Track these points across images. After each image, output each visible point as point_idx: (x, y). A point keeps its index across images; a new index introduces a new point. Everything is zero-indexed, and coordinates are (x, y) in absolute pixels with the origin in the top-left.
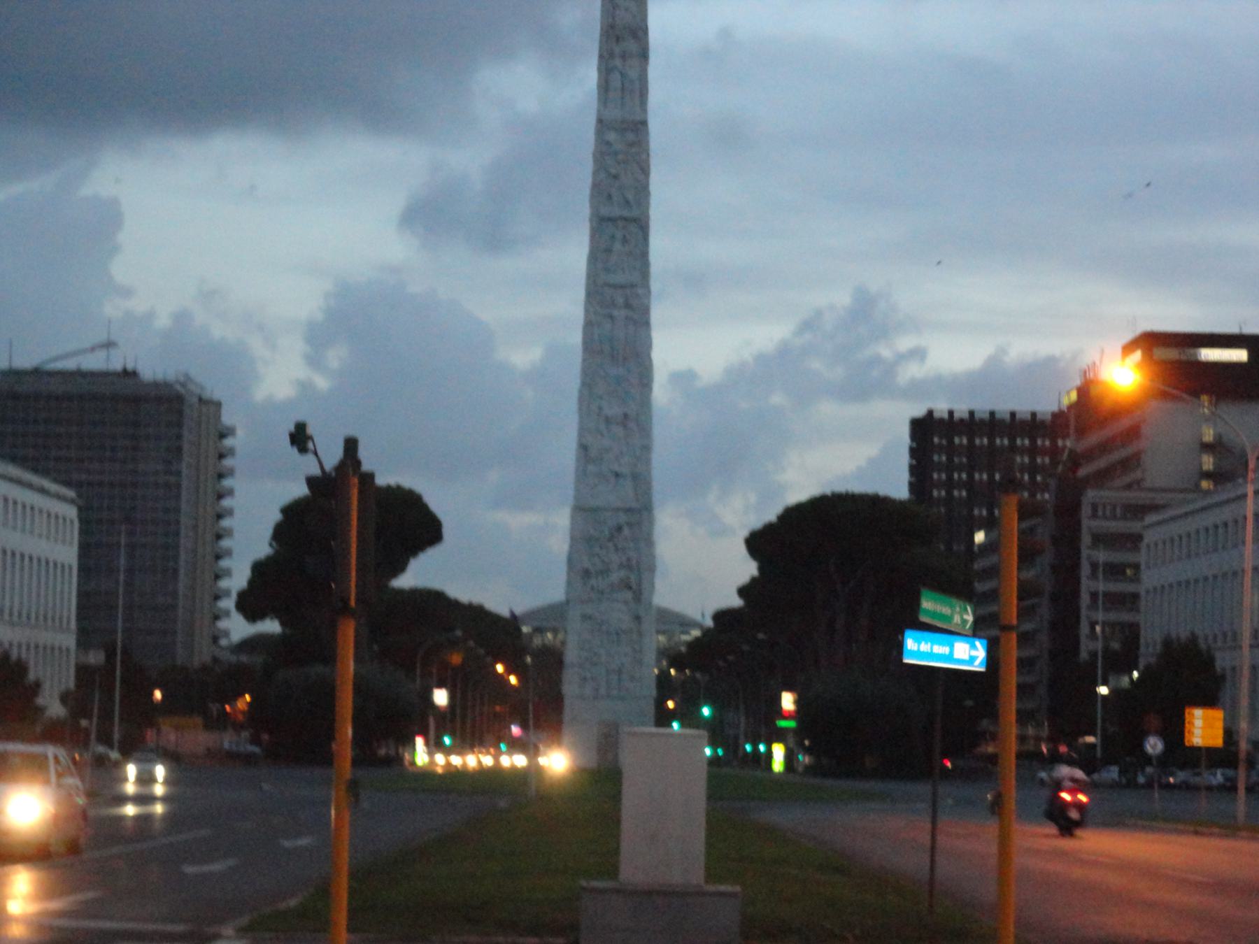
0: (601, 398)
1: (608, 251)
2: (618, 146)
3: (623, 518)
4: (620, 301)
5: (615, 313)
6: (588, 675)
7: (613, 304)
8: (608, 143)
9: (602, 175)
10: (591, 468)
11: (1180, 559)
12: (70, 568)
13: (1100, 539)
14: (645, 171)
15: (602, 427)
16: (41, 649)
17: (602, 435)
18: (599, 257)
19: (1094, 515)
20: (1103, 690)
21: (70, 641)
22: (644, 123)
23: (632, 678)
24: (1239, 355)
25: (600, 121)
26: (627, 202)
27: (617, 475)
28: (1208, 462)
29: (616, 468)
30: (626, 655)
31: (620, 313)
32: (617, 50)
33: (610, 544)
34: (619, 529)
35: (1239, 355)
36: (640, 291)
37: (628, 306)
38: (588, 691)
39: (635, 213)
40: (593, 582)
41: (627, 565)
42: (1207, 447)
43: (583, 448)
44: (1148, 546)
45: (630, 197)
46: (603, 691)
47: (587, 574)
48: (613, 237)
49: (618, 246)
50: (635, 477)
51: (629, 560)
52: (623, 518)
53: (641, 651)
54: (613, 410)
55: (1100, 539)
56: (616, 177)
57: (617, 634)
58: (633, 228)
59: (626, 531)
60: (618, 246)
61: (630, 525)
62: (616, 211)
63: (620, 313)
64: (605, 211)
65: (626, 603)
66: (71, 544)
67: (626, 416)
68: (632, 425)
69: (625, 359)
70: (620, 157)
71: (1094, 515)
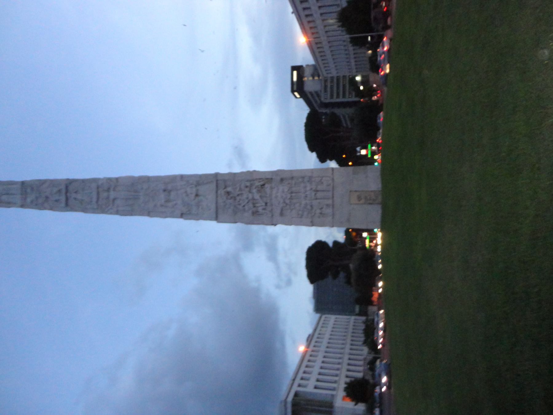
1: (81, 201)
4: (105, 194)
6: (318, 211)
7: (108, 198)
8: (32, 202)
9: (46, 205)
12: (336, 318)
13: (332, 96)
15: (170, 204)
18: (84, 207)
21: (353, 318)
22: (23, 183)
23: (321, 182)
24: (295, 73)
26: (60, 191)
27: (197, 195)
28: (316, 78)
29: (193, 195)
30: (305, 187)
31: (112, 194)
33: (238, 198)
34: (228, 193)
36: (100, 183)
37: (108, 190)
38: (329, 211)
39: (63, 187)
40: (260, 209)
42: (313, 78)
43: (182, 216)
44: (327, 73)
45: (55, 190)
46: (330, 202)
49: (79, 196)
50: (198, 184)
51: (247, 187)
52: (221, 192)
53: (303, 178)
54: (162, 197)
57: (292, 193)
58: (71, 188)
59: (229, 189)
60: (79, 196)
61: (226, 187)
62: (63, 198)
63: (112, 194)
64: (63, 205)
65: (272, 188)
67: (165, 190)
68: (169, 187)
69: (136, 191)
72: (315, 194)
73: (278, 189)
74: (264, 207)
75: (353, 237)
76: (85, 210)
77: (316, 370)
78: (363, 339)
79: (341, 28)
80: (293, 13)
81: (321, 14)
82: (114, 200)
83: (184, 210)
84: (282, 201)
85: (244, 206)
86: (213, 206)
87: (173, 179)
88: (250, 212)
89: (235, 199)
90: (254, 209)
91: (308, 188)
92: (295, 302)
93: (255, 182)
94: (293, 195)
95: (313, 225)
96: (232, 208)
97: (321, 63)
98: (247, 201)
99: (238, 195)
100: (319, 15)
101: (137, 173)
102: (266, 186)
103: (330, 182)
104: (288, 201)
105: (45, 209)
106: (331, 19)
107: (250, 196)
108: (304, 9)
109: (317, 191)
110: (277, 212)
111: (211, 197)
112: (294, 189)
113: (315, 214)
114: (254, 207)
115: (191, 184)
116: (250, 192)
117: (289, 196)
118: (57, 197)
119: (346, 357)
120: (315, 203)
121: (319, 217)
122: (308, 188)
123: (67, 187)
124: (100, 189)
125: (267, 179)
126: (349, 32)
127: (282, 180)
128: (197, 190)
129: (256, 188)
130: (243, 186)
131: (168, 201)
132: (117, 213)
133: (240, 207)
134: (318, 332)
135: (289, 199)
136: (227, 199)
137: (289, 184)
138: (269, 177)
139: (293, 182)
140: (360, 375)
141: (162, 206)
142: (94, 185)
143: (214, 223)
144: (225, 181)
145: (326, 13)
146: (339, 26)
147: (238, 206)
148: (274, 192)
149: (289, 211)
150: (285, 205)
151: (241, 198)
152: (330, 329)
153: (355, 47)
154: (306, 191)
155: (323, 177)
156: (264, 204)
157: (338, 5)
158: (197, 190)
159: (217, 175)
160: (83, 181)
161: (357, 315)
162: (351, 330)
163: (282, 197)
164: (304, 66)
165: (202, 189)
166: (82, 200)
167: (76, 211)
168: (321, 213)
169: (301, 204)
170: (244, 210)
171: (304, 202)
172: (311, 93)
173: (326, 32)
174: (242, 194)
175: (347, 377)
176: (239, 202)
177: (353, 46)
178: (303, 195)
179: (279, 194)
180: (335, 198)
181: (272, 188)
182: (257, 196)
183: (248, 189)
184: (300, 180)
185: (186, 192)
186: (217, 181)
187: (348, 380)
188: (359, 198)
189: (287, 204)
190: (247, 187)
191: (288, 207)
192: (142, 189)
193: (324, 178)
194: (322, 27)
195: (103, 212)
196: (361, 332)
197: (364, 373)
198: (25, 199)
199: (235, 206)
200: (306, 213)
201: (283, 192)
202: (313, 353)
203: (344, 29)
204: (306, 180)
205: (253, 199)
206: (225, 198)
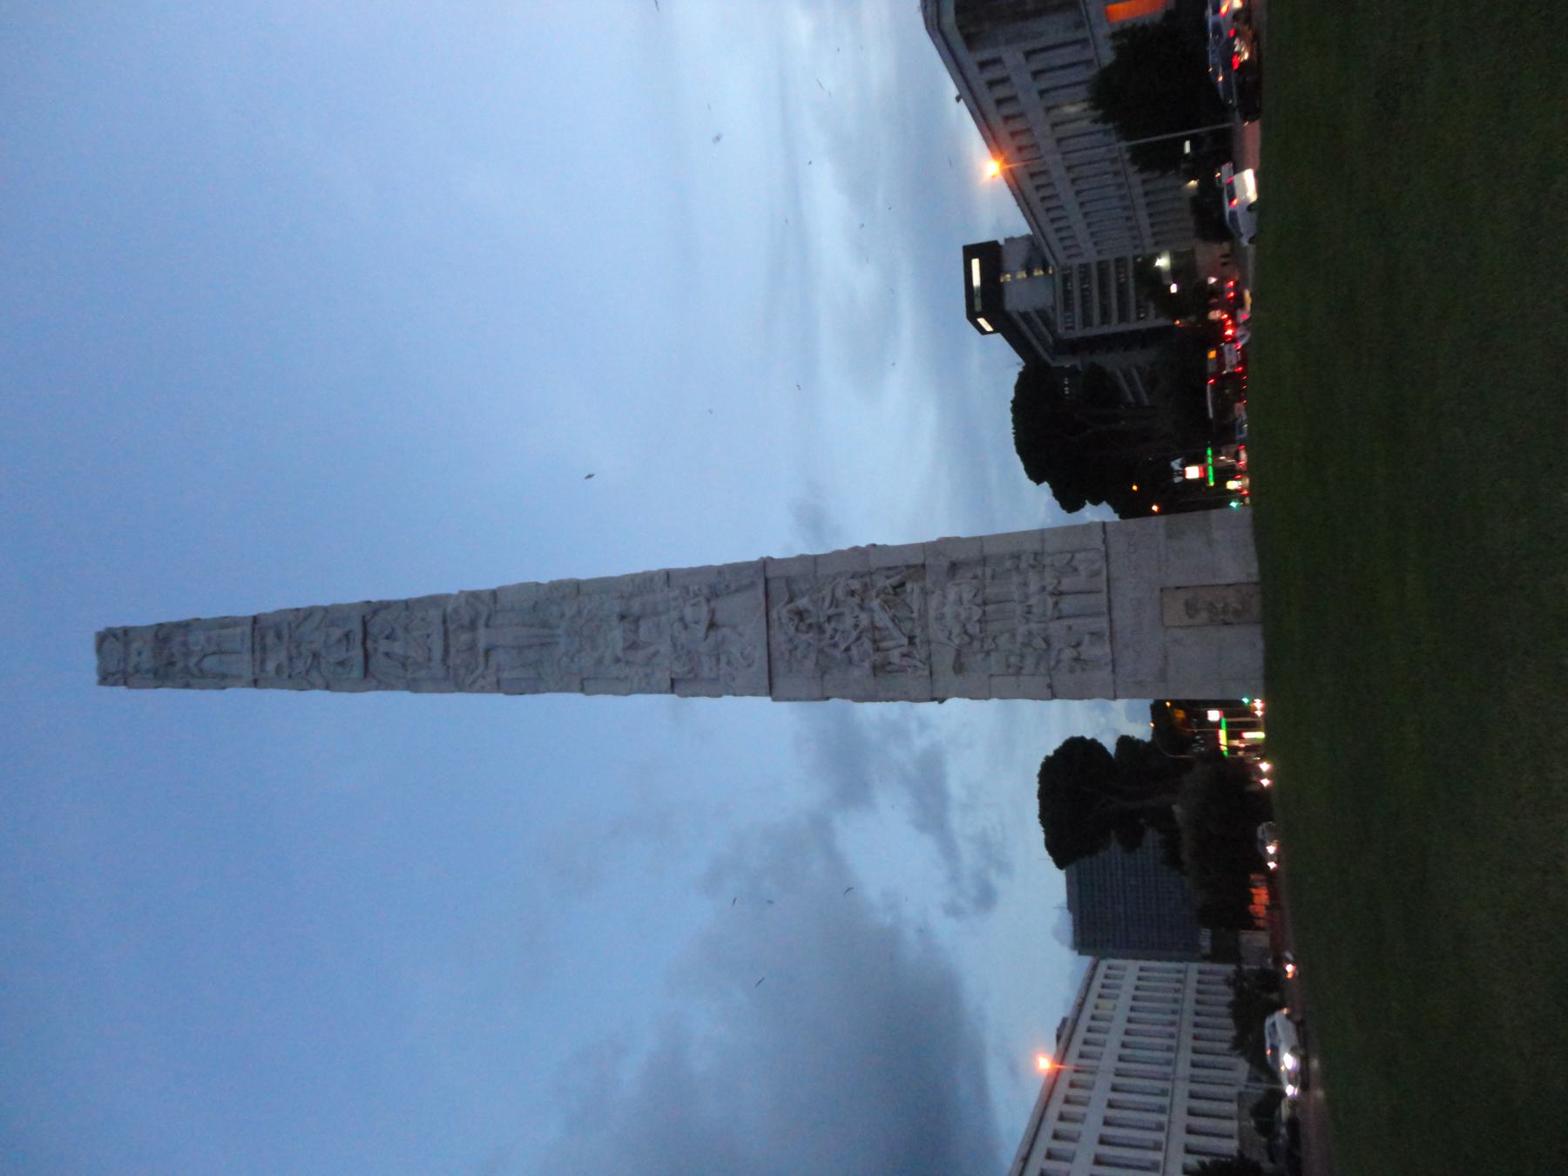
0: (600, 662)
2: (282, 656)
3: (781, 611)
4: (465, 637)
5: (482, 645)
6: (1068, 654)
8: (279, 669)
10: (707, 668)
11: (1077, 246)
12: (1141, 969)
13: (1087, 322)
14: (310, 612)
15: (640, 656)
16: (1202, 987)
17: (656, 654)
19: (1072, 328)
20: (1174, 289)
22: (255, 619)
24: (975, 263)
25: (255, 683)
26: (347, 636)
27: (712, 625)
28: (1038, 273)
29: (702, 628)
30: (1026, 584)
31: (483, 637)
32: (180, 665)
33: (829, 628)
34: (800, 614)
35: (975, 263)
36: (449, 609)
37: (473, 626)
38: (1101, 651)
40: (895, 656)
41: (861, 597)
42: (1029, 272)
43: (673, 686)
44: (1069, 257)
45: (337, 633)
47: (875, 669)
48: (387, 654)
49: (397, 648)
50: (714, 594)
52: (781, 611)
53: (1017, 557)
54: (617, 635)
55: (1087, 322)
56: (315, 655)
57: (985, 603)
59: (803, 602)
60: (397, 648)
61: (791, 600)
62: (357, 653)
63: (483, 637)
64: (357, 672)
65: (925, 593)
66: (1125, 969)
68: (636, 606)
69: (545, 625)
70: (294, 652)
71: (1072, 328)
72: (1056, 604)
73: (945, 597)
74: (904, 650)
75: (1178, 724)
76: (413, 686)
77: (1092, 1127)
78: (1233, 1033)
79: (1099, 126)
80: (958, 99)
81: (1042, 93)
82: (487, 652)
83: (679, 670)
84: (957, 630)
85: (848, 649)
86: (760, 654)
87: (643, 583)
88: (867, 664)
89: (821, 630)
90: (878, 657)
91: (1033, 587)
92: (1014, 958)
93: (875, 577)
94: (989, 608)
95: (1054, 696)
96: (813, 656)
97: (1049, 229)
98: (855, 634)
99: (829, 619)
100: (1035, 96)
101: (546, 575)
102: (909, 587)
103: (1100, 564)
104: (974, 629)
105: (313, 686)
106: (1072, 104)
107: (864, 620)
108: (992, 84)
109: (1061, 593)
110: (945, 660)
111: (752, 629)
112: (991, 591)
113: (1058, 662)
114: (878, 650)
115: (696, 595)
116: (861, 607)
117: (977, 613)
118: (343, 655)
119: (1182, 1089)
120: (1056, 628)
121: (1072, 671)
122: (1033, 587)
123: (365, 624)
124: (451, 627)
125: (908, 567)
126: (1126, 132)
127: (954, 567)
128: (713, 612)
129: (877, 596)
130: (840, 593)
131: (632, 646)
132: (499, 687)
133: (838, 654)
134: (1088, 1010)
135: (979, 621)
136: (797, 629)
137: (975, 577)
138: (917, 560)
139: (989, 571)
140: (1230, 1146)
141: (617, 660)
142: (435, 615)
143: (767, 700)
144: (789, 581)
145: (1055, 88)
146: (1095, 121)
147: (829, 650)
148: (934, 602)
149: (980, 657)
150: (967, 639)
151: (837, 625)
152: (1125, 1000)
153: (1145, 176)
154: (1027, 597)
155: (1073, 553)
156: (905, 641)
157: (1088, 63)
158: (713, 612)
159: (765, 563)
160: (407, 604)
161: (1205, 958)
162: (1189, 1006)
163: (957, 616)
164: (1001, 242)
165: (729, 608)
166: (407, 658)
167: (389, 687)
168: (1077, 659)
169: (1013, 636)
170: (850, 661)
171: (1022, 629)
172: (1025, 316)
173: (1059, 141)
174: (840, 615)
175: (1189, 1150)
176: (832, 637)
177: (1141, 171)
178: (1019, 609)
179: (948, 611)
180: (1116, 613)
181: (925, 593)
182: (883, 619)
183: (857, 600)
184: (1008, 564)
185: (682, 619)
186: (767, 581)
187: (1192, 1161)
188: (1191, 609)
189: (972, 637)
190: (852, 593)
191: (976, 644)
192: (562, 615)
193: (1078, 556)
194: (1047, 128)
195: (460, 687)
196: (1224, 1010)
197: (1242, 1141)
198: (263, 661)
199: (821, 651)
200: (1029, 662)
201: (960, 601)
202: (1076, 1077)
203: (1110, 126)
204: (1023, 565)
205: (874, 628)
206: (792, 629)
